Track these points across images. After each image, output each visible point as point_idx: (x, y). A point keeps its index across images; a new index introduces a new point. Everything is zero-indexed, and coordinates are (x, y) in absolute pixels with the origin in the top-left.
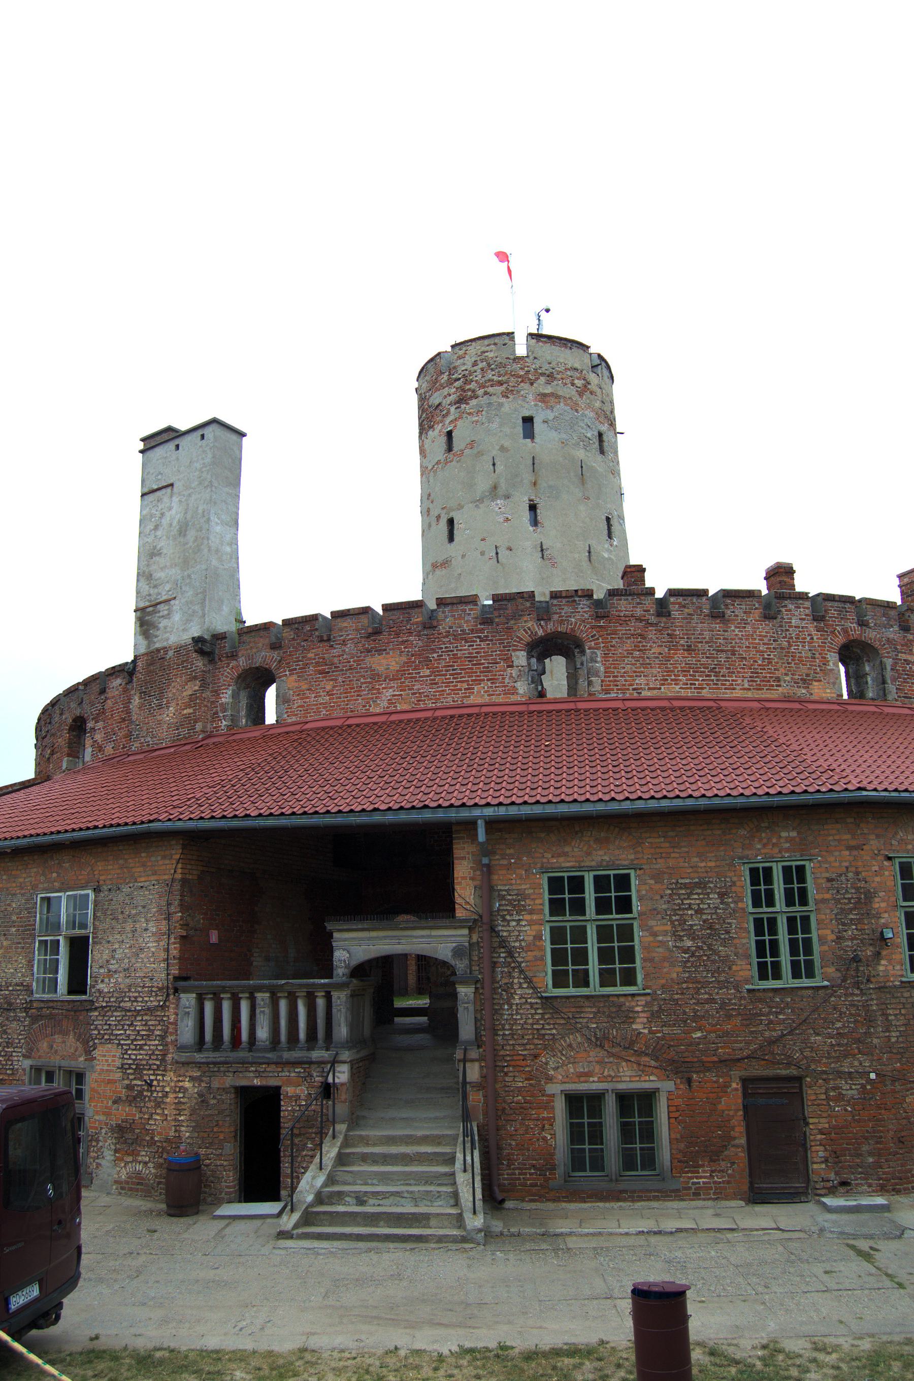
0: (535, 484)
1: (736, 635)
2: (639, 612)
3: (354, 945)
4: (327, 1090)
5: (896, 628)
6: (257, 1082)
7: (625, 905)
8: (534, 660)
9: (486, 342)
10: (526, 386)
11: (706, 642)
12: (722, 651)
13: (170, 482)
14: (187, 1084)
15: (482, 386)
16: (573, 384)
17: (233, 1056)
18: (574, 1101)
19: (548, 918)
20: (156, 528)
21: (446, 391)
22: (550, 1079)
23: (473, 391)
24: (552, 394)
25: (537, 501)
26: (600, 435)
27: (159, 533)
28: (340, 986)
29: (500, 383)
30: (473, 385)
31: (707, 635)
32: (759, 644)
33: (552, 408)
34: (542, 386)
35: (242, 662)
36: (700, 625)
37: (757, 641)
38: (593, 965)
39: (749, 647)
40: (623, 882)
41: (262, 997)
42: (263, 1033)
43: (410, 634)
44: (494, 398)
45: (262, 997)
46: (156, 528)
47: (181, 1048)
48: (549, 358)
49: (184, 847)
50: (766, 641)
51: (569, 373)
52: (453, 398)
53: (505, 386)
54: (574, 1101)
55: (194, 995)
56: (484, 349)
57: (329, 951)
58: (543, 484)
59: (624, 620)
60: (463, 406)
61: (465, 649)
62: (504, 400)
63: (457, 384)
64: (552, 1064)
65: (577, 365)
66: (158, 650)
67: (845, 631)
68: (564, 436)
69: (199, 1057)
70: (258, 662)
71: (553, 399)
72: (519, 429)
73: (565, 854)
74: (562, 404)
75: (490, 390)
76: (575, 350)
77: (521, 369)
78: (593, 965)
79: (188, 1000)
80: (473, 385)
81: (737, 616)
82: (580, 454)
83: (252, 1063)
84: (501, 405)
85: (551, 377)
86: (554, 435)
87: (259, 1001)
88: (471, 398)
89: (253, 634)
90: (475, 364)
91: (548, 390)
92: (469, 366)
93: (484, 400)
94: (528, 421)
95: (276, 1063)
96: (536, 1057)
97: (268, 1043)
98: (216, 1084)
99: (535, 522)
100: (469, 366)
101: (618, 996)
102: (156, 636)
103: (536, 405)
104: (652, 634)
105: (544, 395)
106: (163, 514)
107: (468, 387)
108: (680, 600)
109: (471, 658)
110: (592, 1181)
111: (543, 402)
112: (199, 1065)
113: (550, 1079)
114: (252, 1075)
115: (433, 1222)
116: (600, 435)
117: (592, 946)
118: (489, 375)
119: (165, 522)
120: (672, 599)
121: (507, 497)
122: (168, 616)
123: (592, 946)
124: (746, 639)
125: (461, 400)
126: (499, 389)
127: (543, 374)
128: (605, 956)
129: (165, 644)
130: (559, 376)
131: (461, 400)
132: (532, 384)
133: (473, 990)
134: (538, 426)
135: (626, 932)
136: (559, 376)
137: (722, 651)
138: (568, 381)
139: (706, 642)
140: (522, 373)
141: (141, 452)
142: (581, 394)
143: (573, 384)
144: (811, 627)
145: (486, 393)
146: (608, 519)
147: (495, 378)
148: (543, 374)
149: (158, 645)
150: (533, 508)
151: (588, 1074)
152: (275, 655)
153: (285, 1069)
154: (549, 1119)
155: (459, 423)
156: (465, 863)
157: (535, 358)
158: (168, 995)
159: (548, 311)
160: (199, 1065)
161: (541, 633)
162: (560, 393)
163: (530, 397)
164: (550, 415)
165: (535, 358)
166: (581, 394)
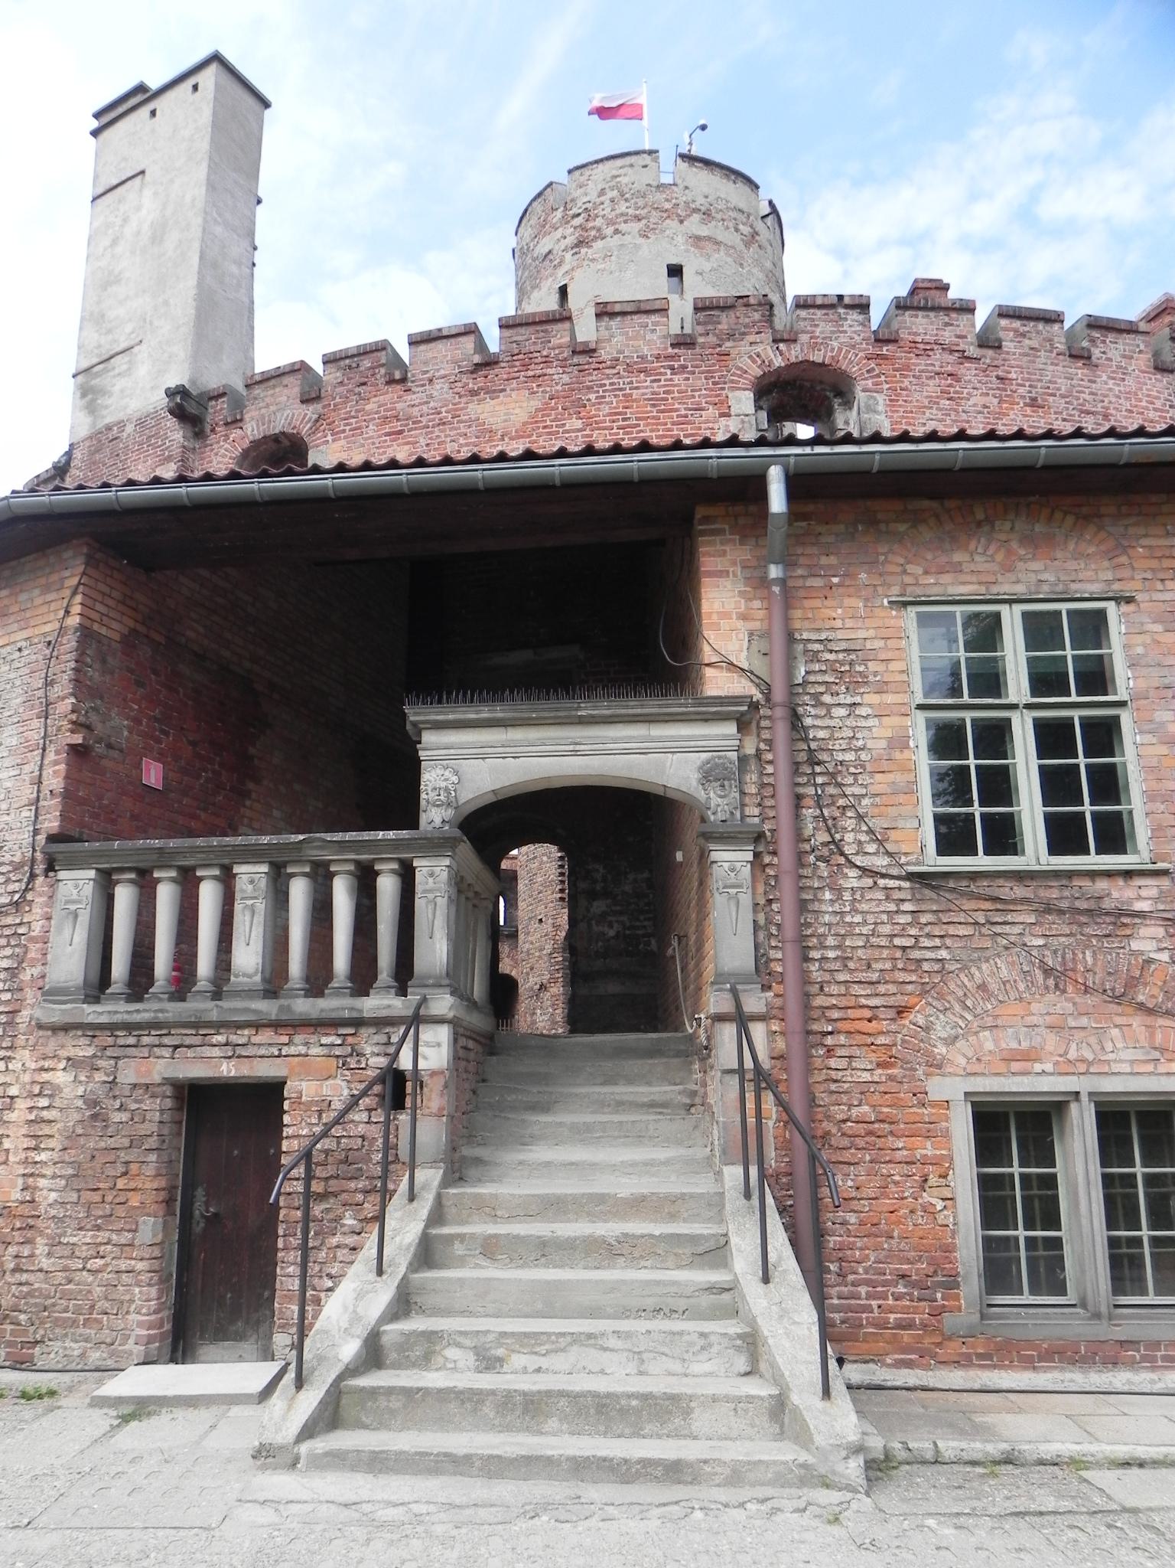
1: (1110, 389)
2: (948, 336)
3: (469, 759)
4: (396, 1088)
6: (228, 1070)
7: (1096, 678)
8: (763, 415)
9: (619, 162)
10: (673, 224)
11: (1063, 396)
12: (1088, 413)
13: (139, 170)
14: (61, 1078)
15: (611, 222)
16: (737, 230)
17: (173, 1010)
18: (994, 1123)
19: (920, 700)
20: (115, 242)
21: (559, 233)
22: (936, 1066)
23: (599, 230)
24: (709, 239)
27: (119, 250)
28: (435, 845)
30: (599, 222)
31: (1063, 385)
32: (1147, 408)
33: (708, 257)
35: (252, 429)
36: (1051, 368)
37: (1144, 404)
38: (1030, 808)
39: (1131, 411)
40: (1092, 627)
41: (251, 876)
42: (248, 957)
43: (547, 362)
44: (628, 239)
45: (251, 876)
46: (115, 242)
47: (53, 994)
48: (706, 190)
49: (91, 562)
50: (1158, 404)
52: (571, 240)
53: (644, 222)
54: (994, 1123)
55: (92, 874)
56: (615, 172)
57: (413, 768)
59: (924, 350)
60: (584, 250)
61: (646, 386)
62: (642, 240)
63: (577, 221)
64: (941, 1030)
66: (109, 428)
69: (93, 1013)
70: (279, 425)
71: (709, 246)
73: (957, 569)
74: (722, 253)
75: (623, 227)
76: (740, 185)
77: (667, 200)
78: (1030, 808)
79: (77, 885)
80: (599, 222)
81: (1110, 360)
83: (220, 1026)
84: (637, 247)
87: (242, 885)
88: (595, 238)
89: (273, 382)
90: (602, 192)
91: (704, 231)
92: (593, 196)
93: (613, 242)
95: (276, 1025)
96: (901, 1011)
97: (258, 978)
98: (129, 1074)
100: (593, 196)
101: (1093, 875)
102: (106, 407)
103: (687, 251)
104: (968, 371)
106: (126, 220)
107: (590, 224)
108: (1017, 324)
109: (655, 401)
110: (1047, 1316)
111: (697, 247)
112: (91, 1030)
113: (936, 1066)
114: (216, 1052)
115: (701, 1420)
117: (1025, 762)
118: (622, 207)
119: (129, 231)
120: (1004, 322)
122: (128, 372)
123: (1025, 762)
124: (1127, 399)
125: (580, 243)
126: (635, 227)
127: (696, 210)
128: (1057, 785)
129: (121, 416)
130: (719, 216)
131: (580, 243)
132: (681, 222)
133: (750, 856)
135: (1104, 735)
136: (719, 216)
137: (1088, 413)
138: (731, 225)
139: (1063, 396)
140: (667, 206)
141: (95, 133)
143: (737, 230)
145: (617, 232)
147: (631, 211)
148: (696, 210)
149: (108, 420)
151: (1029, 1056)
152: (311, 411)
153: (298, 1039)
154: (936, 1162)
155: (577, 274)
156: (727, 583)
157: (687, 188)
158: (33, 876)
159: (703, 128)
160: (91, 1030)
161: (779, 362)
162: (720, 238)
163: (680, 239)
165: (687, 188)
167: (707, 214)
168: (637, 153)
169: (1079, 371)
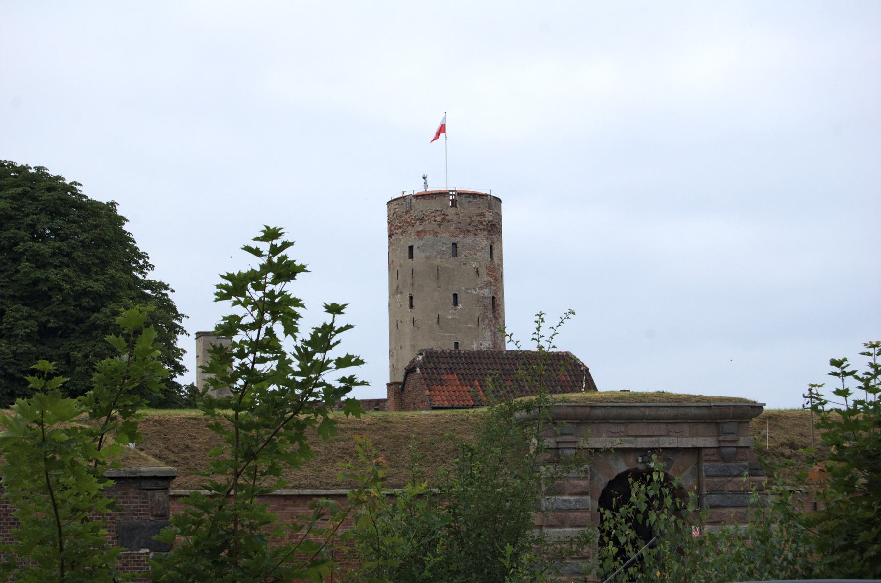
9: (396, 202)
16: (435, 221)
24: (423, 230)
25: (413, 294)
26: (455, 245)
29: (400, 227)
58: (416, 284)
62: (401, 237)
68: (428, 254)
71: (423, 234)
72: (407, 254)
82: (438, 262)
85: (422, 220)
86: (423, 255)
94: (411, 248)
99: (411, 306)
105: (419, 232)
111: (418, 236)
134: (415, 251)
142: (439, 226)
146: (455, 295)
150: (411, 298)
163: (412, 234)
164: (421, 243)
166: (439, 226)
167: (422, 220)
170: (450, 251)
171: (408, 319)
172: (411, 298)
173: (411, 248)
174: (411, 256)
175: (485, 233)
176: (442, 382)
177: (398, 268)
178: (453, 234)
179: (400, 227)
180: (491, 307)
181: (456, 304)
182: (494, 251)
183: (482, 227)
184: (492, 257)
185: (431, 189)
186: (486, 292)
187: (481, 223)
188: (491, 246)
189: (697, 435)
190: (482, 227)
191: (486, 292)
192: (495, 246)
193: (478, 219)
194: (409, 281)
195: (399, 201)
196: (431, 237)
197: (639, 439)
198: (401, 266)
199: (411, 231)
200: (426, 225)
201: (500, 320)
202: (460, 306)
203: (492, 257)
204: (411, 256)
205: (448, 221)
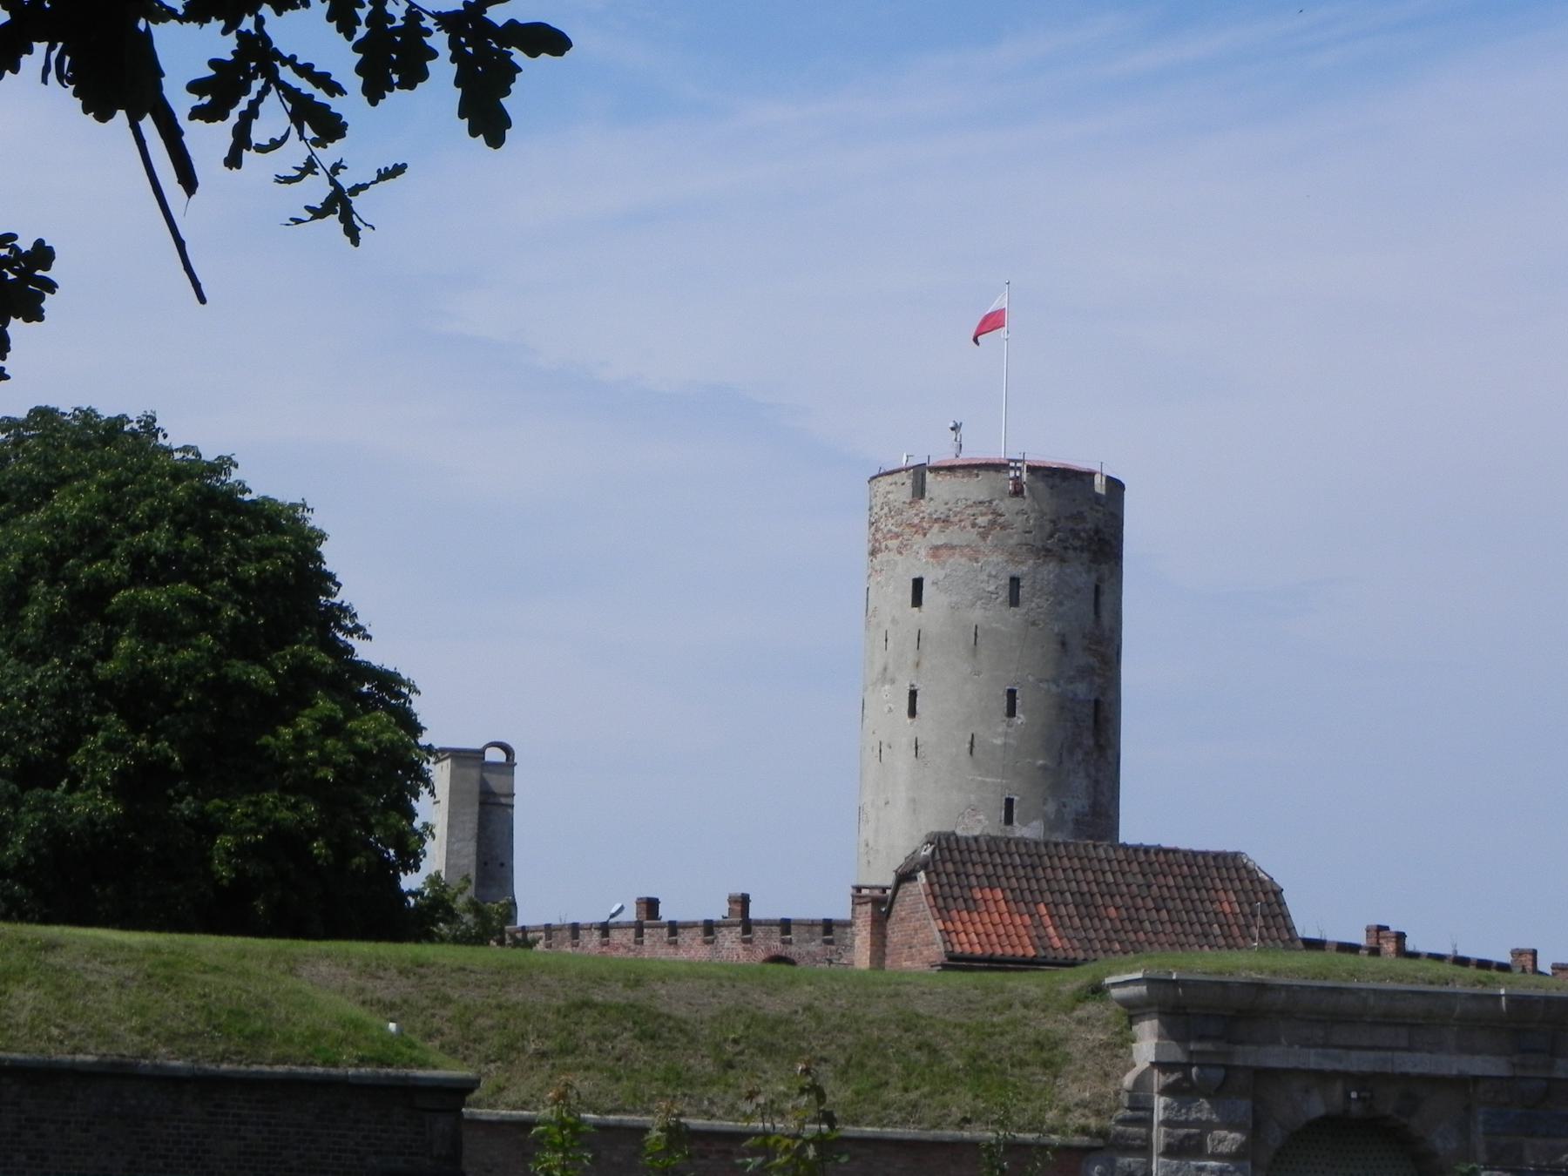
0: (918, 665)
2: (625, 941)
5: (819, 942)
9: (889, 479)
10: (918, 537)
16: (974, 525)
24: (945, 546)
29: (897, 536)
34: (936, 537)
48: (946, 497)
51: (970, 511)
58: (925, 664)
62: (898, 557)
65: (981, 498)
67: (769, 949)
71: (944, 552)
94: (918, 584)
99: (912, 712)
105: (937, 548)
111: (934, 556)
116: (1015, 582)
121: (893, 681)
127: (936, 520)
138: (967, 523)
140: (916, 521)
142: (984, 536)
144: (740, 951)
146: (1011, 694)
147: (894, 529)
148: (936, 520)
150: (913, 694)
163: (923, 552)
164: (941, 574)
166: (984, 536)
168: (899, 471)
169: (671, 950)
170: (1004, 594)
171: (905, 743)
172: (913, 694)
173: (918, 584)
174: (917, 600)
175: (1085, 555)
176: (971, 905)
177: (887, 625)
178: (1012, 556)
179: (897, 536)
180: (1090, 722)
181: (1011, 712)
182: (1103, 599)
183: (1077, 543)
184: (1097, 612)
185: (967, 456)
186: (1081, 689)
187: (1075, 534)
188: (1097, 590)
189: (1473, 1051)
190: (1077, 543)
191: (1081, 689)
192: (1105, 587)
193: (1071, 525)
194: (911, 656)
195: (896, 477)
196: (963, 560)
197: (1354, 1054)
198: (894, 621)
199: (921, 545)
200: (953, 535)
201: (1110, 752)
202: (1020, 718)
203: (1097, 612)
204: (917, 600)
205: (1003, 527)
